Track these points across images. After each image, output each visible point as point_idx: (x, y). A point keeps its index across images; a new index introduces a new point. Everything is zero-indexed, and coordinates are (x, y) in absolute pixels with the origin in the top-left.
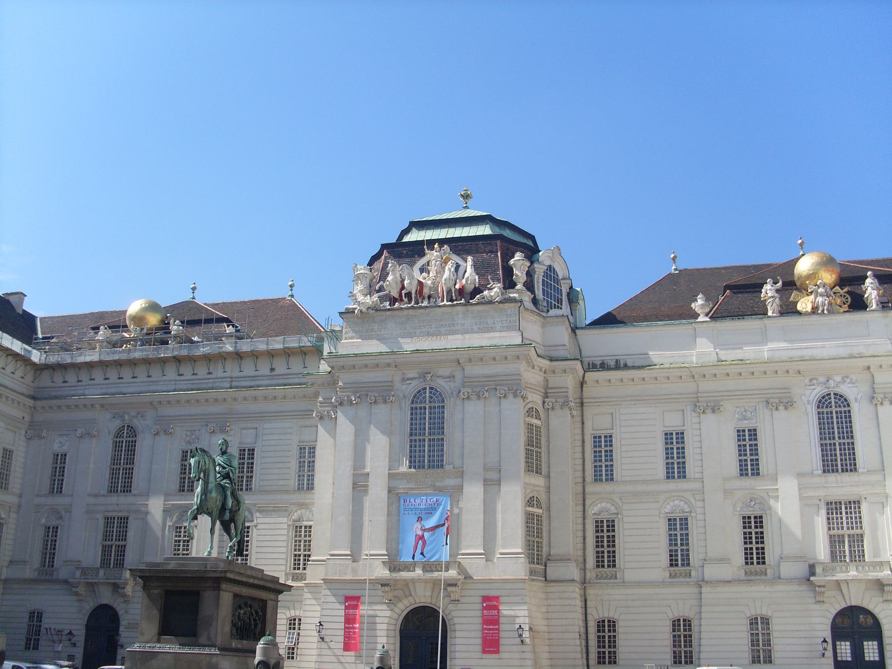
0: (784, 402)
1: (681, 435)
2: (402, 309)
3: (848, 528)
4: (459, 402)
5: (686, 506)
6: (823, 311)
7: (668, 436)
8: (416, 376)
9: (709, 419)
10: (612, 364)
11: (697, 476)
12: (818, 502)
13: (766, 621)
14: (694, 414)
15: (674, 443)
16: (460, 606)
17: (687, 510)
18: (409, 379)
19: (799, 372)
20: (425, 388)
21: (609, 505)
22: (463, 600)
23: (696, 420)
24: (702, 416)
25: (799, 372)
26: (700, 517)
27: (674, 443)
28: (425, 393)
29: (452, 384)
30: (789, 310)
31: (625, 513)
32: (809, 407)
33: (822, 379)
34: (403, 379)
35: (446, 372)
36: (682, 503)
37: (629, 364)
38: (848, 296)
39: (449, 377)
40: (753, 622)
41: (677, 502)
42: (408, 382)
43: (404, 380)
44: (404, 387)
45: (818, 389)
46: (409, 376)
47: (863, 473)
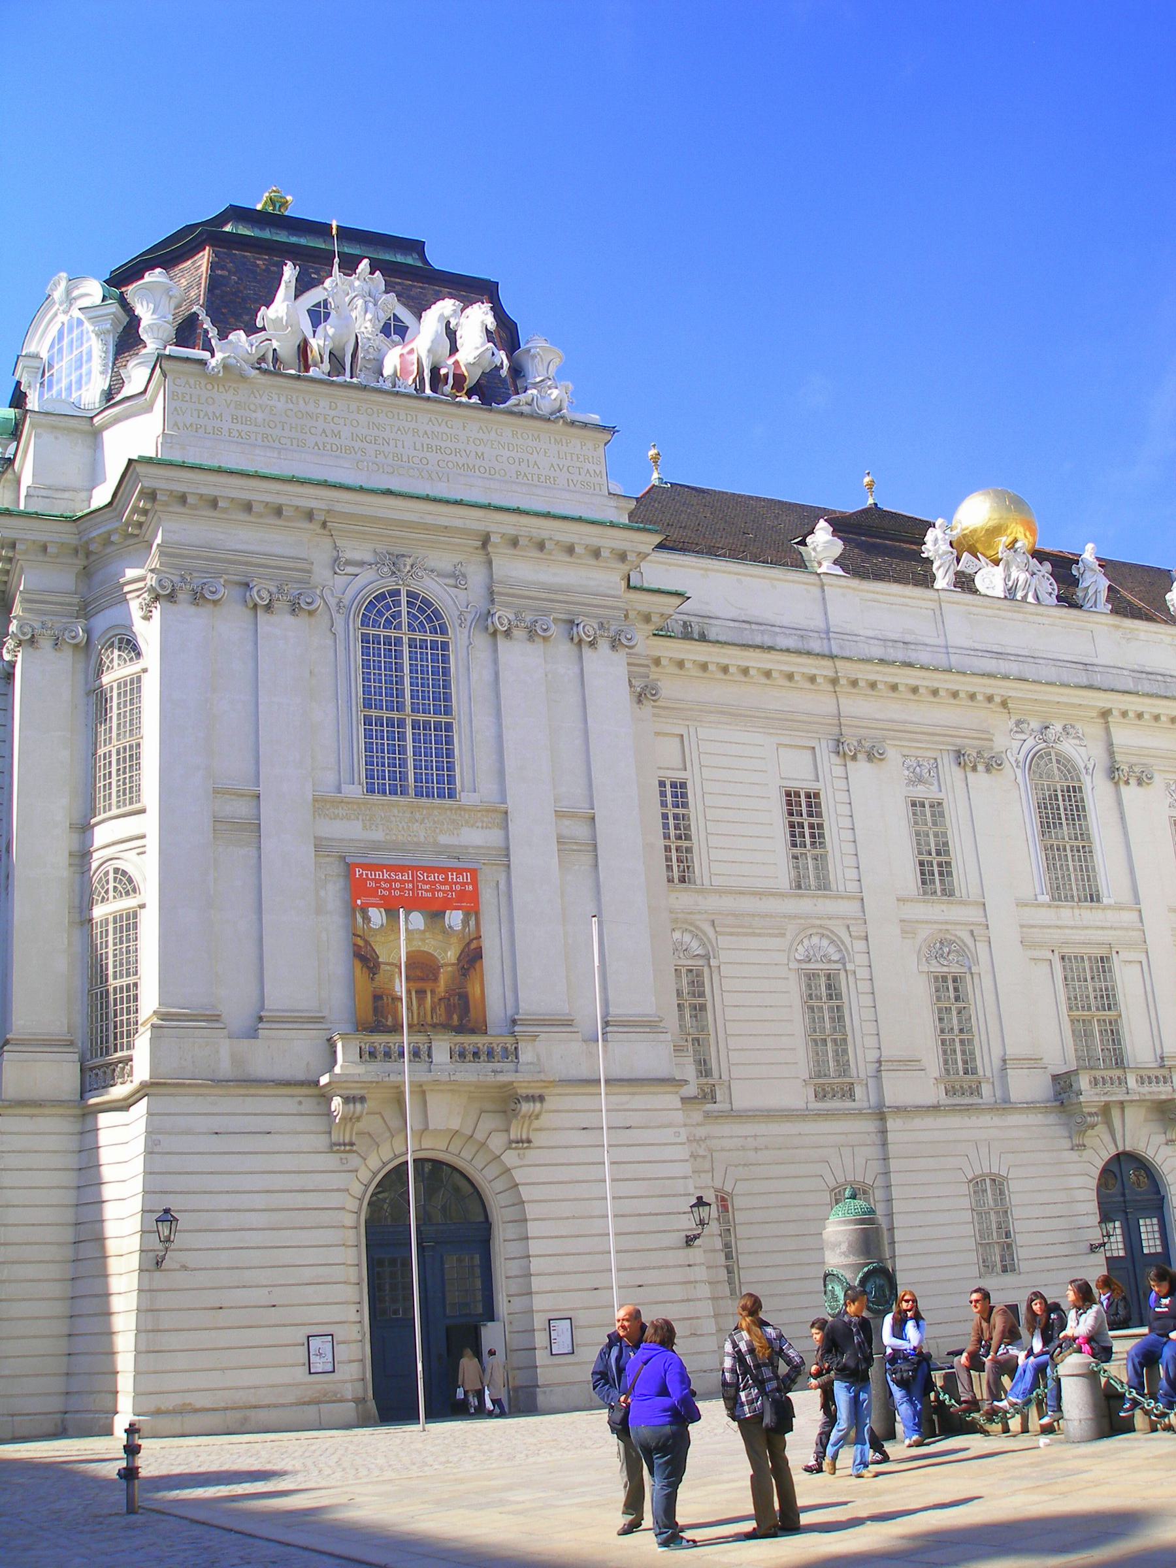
0: (974, 758)
1: (813, 798)
2: (333, 383)
3: (1098, 1009)
4: (481, 641)
5: (831, 950)
6: (1026, 596)
7: (791, 797)
8: (368, 557)
9: (861, 769)
10: (678, 629)
11: (852, 887)
12: (1049, 955)
13: (998, 1183)
14: (835, 759)
15: (803, 814)
16: (532, 1155)
17: (835, 957)
18: (348, 563)
19: (1004, 704)
20: (397, 593)
21: (687, 938)
22: (538, 1139)
23: (839, 771)
24: (850, 764)
25: (1004, 704)
26: (862, 973)
27: (803, 814)
28: (397, 603)
29: (462, 594)
30: (965, 582)
31: (724, 956)
32: (1019, 772)
33: (1035, 724)
34: (336, 560)
35: (443, 560)
36: (825, 942)
37: (712, 634)
38: (1052, 580)
39: (453, 575)
40: (977, 1184)
41: (815, 940)
42: (350, 570)
43: (337, 563)
44: (340, 580)
45: (1030, 742)
46: (348, 555)
47: (1109, 907)
